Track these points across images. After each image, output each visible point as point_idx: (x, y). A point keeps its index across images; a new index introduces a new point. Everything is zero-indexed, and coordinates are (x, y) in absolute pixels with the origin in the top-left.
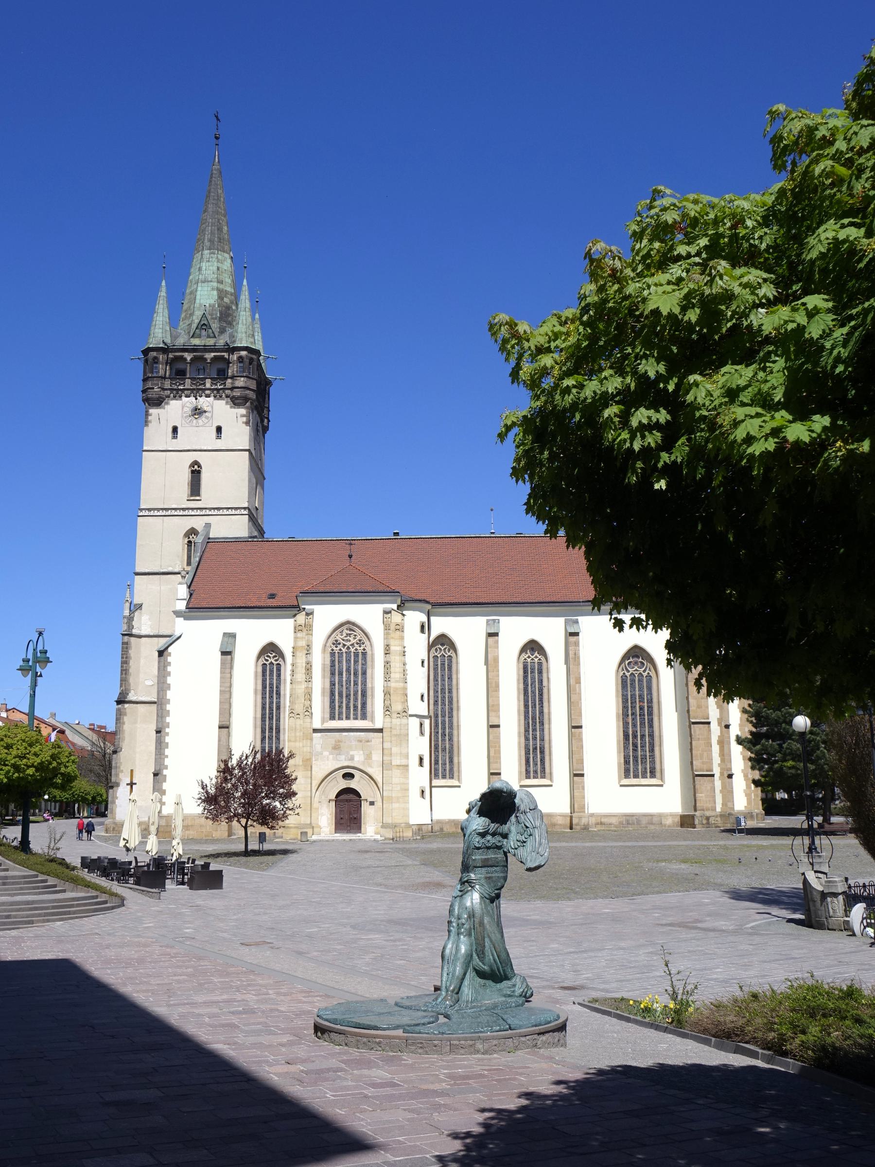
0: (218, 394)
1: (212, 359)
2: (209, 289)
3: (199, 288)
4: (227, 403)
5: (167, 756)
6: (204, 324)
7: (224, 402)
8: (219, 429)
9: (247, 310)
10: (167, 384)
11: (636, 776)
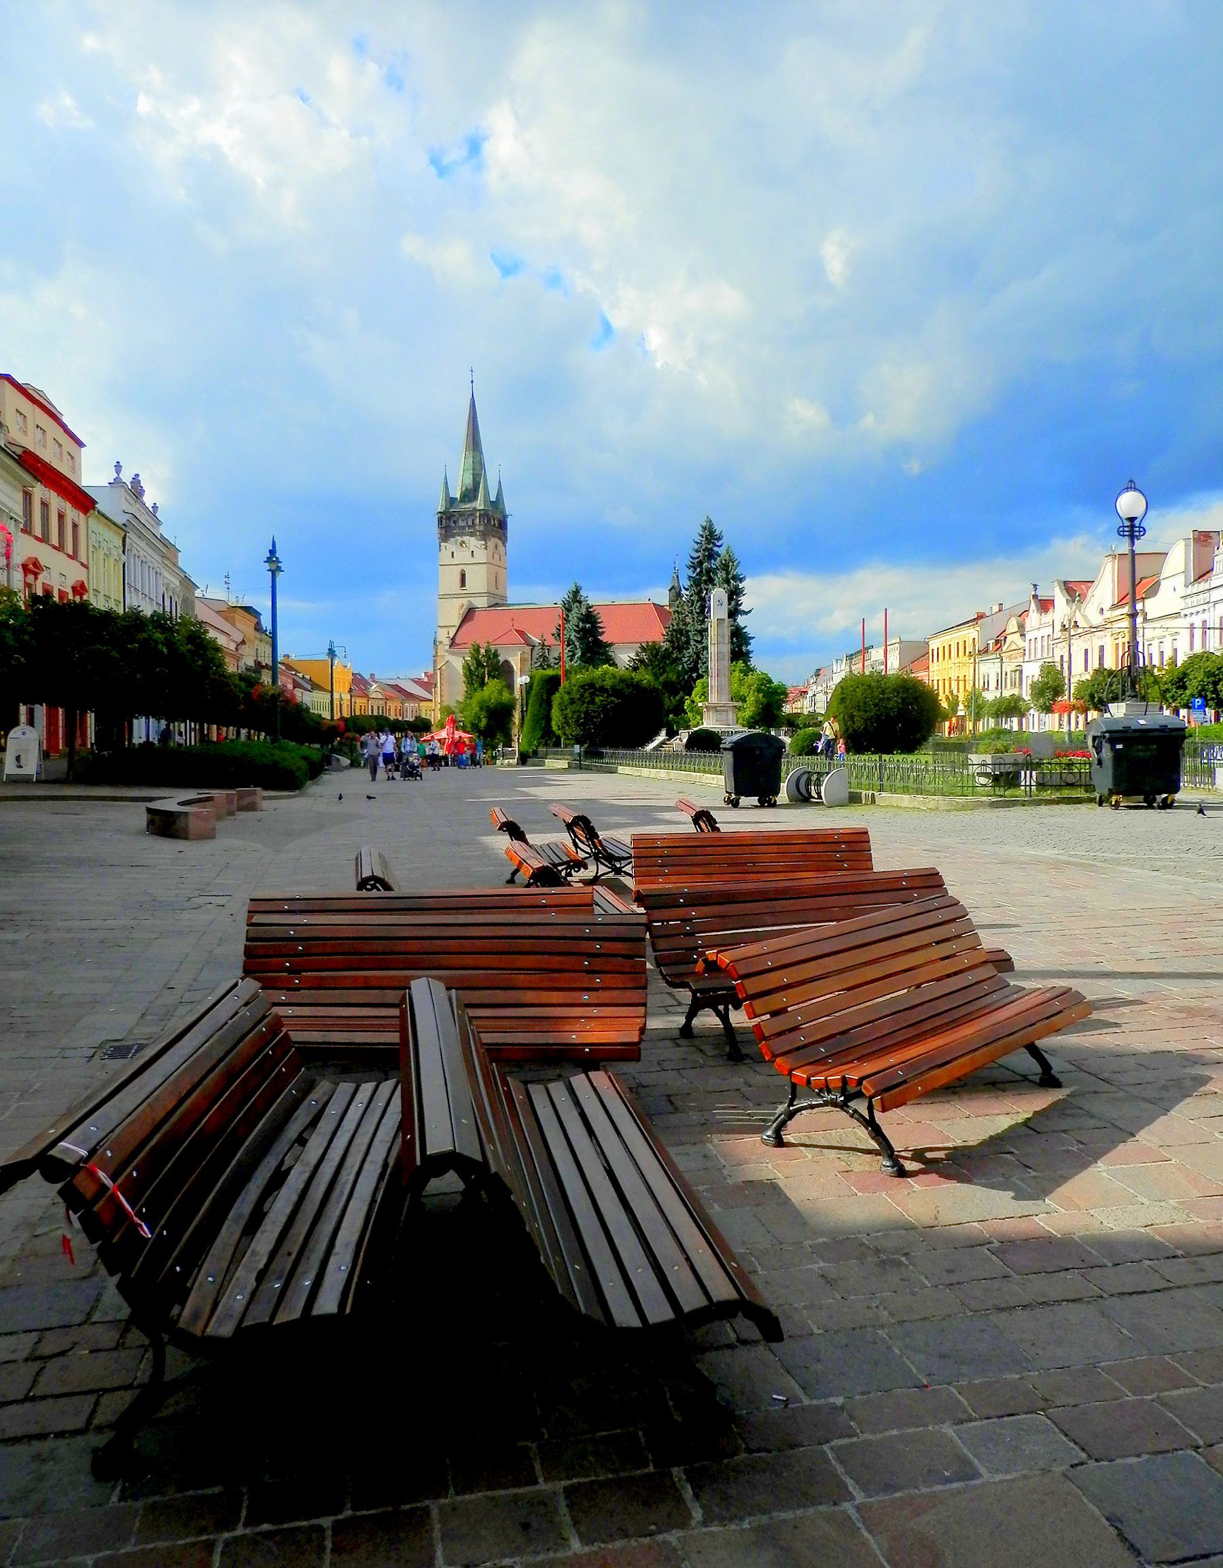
0: (472, 535)
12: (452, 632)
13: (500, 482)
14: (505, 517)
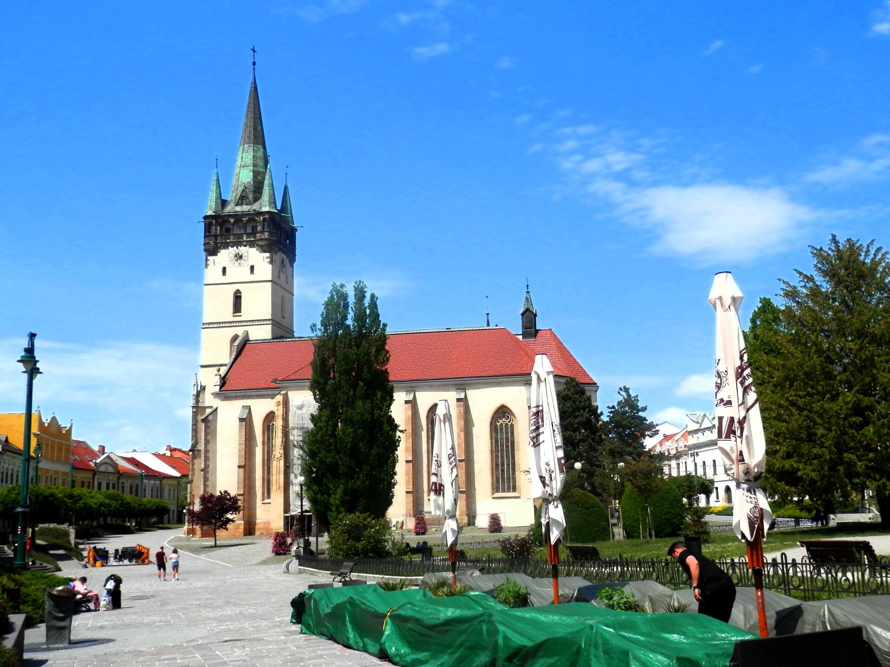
0: (251, 244)
1: (247, 221)
2: (248, 171)
3: (241, 171)
4: (257, 250)
5: (208, 486)
6: (244, 196)
8: (252, 268)
11: (503, 491)
12: (223, 370)
13: (286, 188)
14: (294, 230)
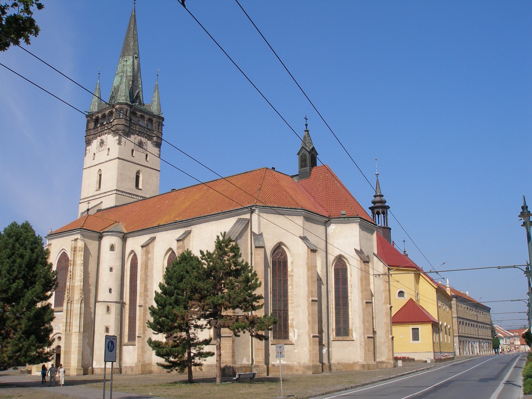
1: (108, 113)
7: (111, 135)
8: (109, 149)
9: (123, 83)
10: (92, 132)
